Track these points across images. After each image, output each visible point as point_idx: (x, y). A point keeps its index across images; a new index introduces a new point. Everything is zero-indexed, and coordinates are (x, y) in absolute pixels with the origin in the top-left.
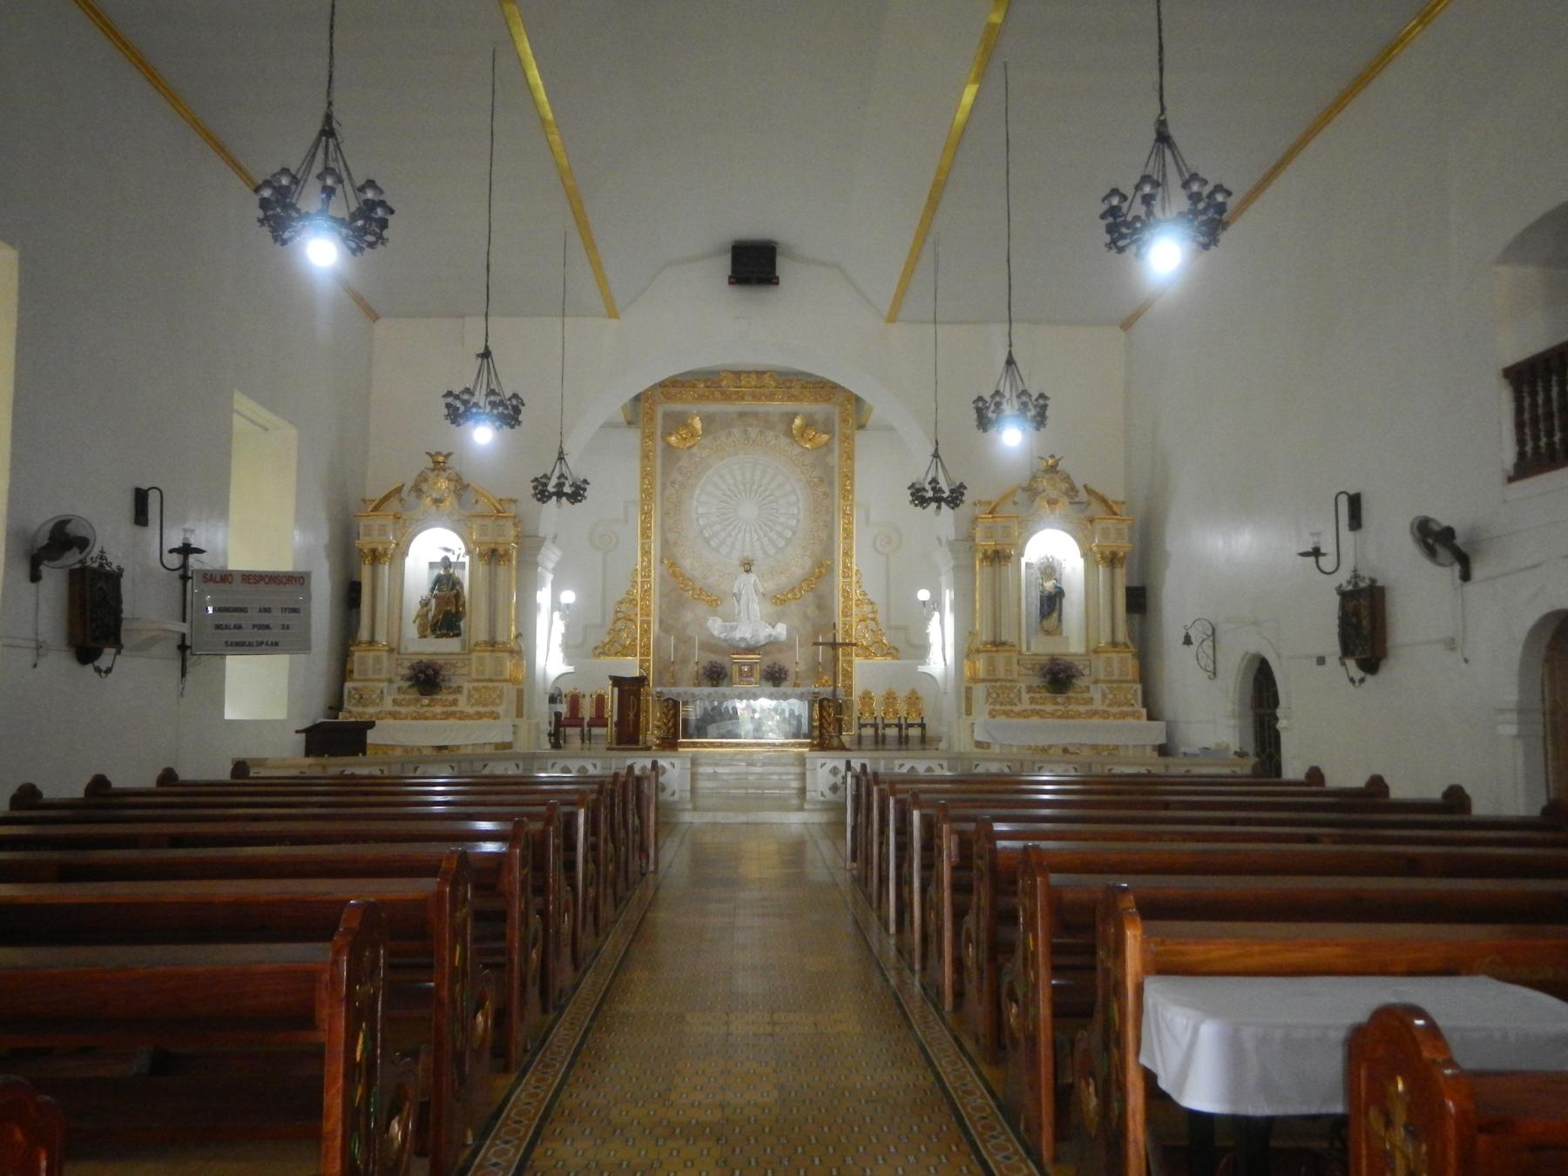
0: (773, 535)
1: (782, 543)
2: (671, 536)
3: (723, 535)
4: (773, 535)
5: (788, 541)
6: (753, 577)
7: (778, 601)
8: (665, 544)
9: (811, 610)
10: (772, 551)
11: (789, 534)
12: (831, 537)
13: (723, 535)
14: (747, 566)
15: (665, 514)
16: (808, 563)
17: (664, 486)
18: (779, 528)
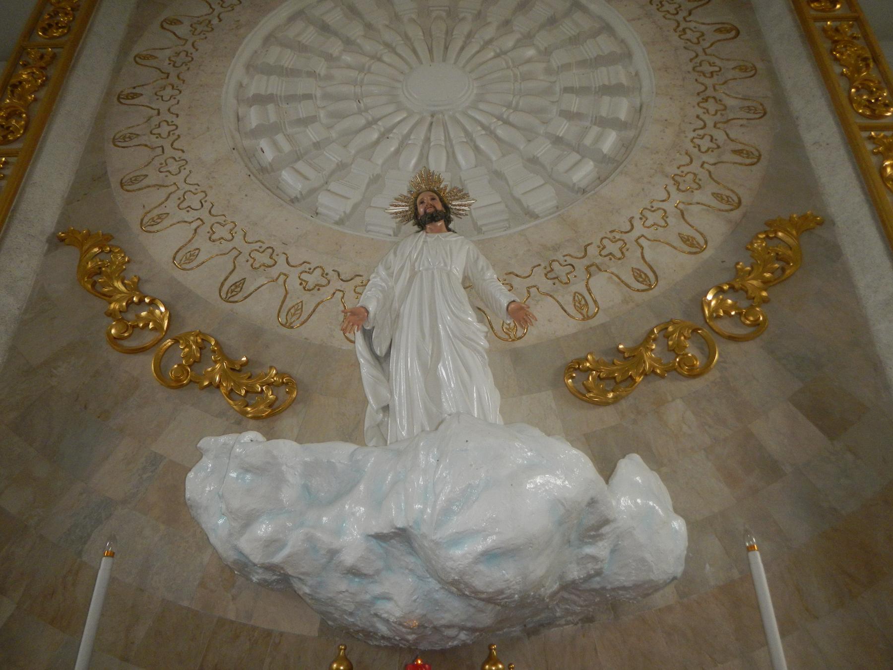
0: (543, 149)
1: (585, 172)
2: (122, 161)
3: (333, 156)
4: (543, 149)
5: (610, 165)
6: (450, 254)
7: (599, 385)
8: (91, 180)
9: (778, 430)
10: (542, 199)
11: (610, 141)
12: (789, 142)
13: (333, 156)
14: (432, 211)
15: (120, 97)
16: (714, 228)
17: (135, 30)
18: (563, 128)
